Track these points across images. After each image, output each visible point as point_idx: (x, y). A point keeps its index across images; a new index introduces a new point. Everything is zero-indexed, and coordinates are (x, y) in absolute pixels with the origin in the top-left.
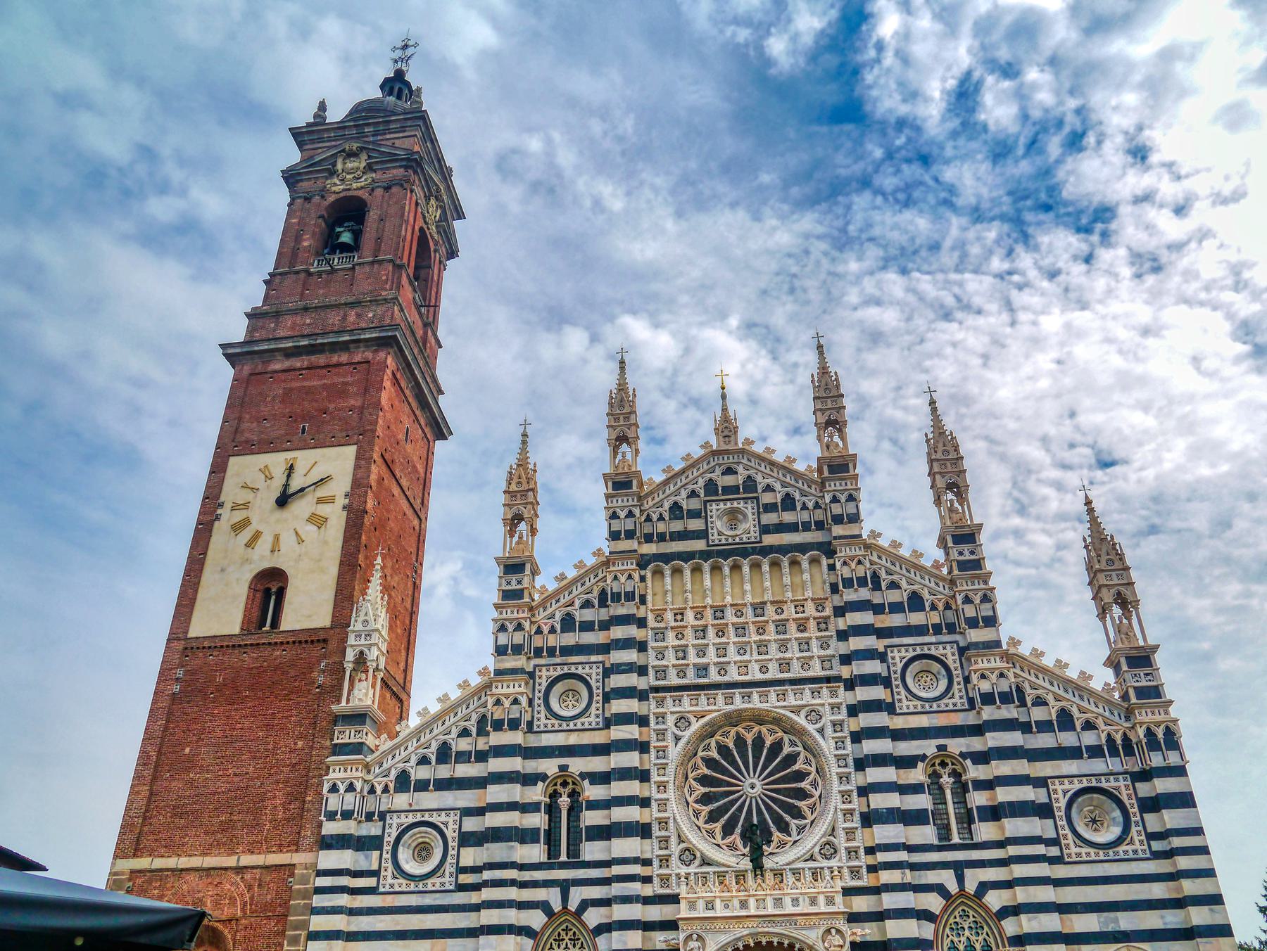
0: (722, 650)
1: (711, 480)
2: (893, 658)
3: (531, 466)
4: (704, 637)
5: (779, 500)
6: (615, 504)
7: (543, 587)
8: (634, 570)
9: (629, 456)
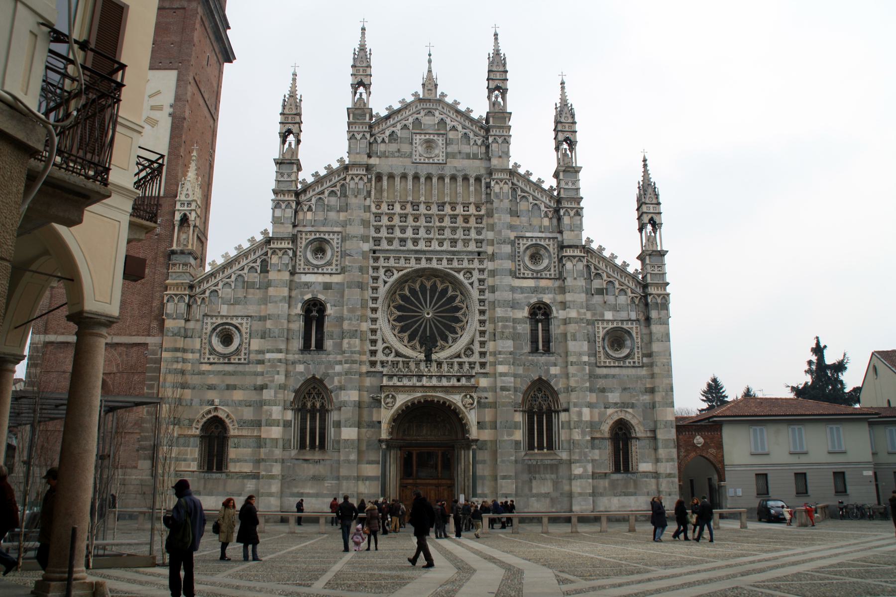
0: (416, 230)
1: (417, 119)
2: (519, 244)
3: (298, 97)
4: (405, 222)
5: (460, 137)
6: (354, 129)
7: (304, 180)
8: (365, 175)
9: (364, 96)
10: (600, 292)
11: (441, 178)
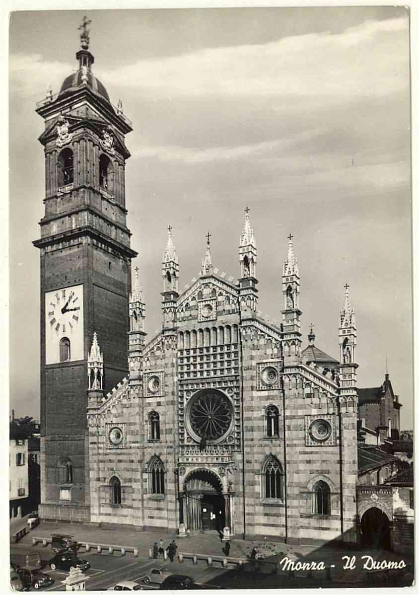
1: (200, 291)
2: (259, 368)
10: (309, 396)
11: (215, 329)
